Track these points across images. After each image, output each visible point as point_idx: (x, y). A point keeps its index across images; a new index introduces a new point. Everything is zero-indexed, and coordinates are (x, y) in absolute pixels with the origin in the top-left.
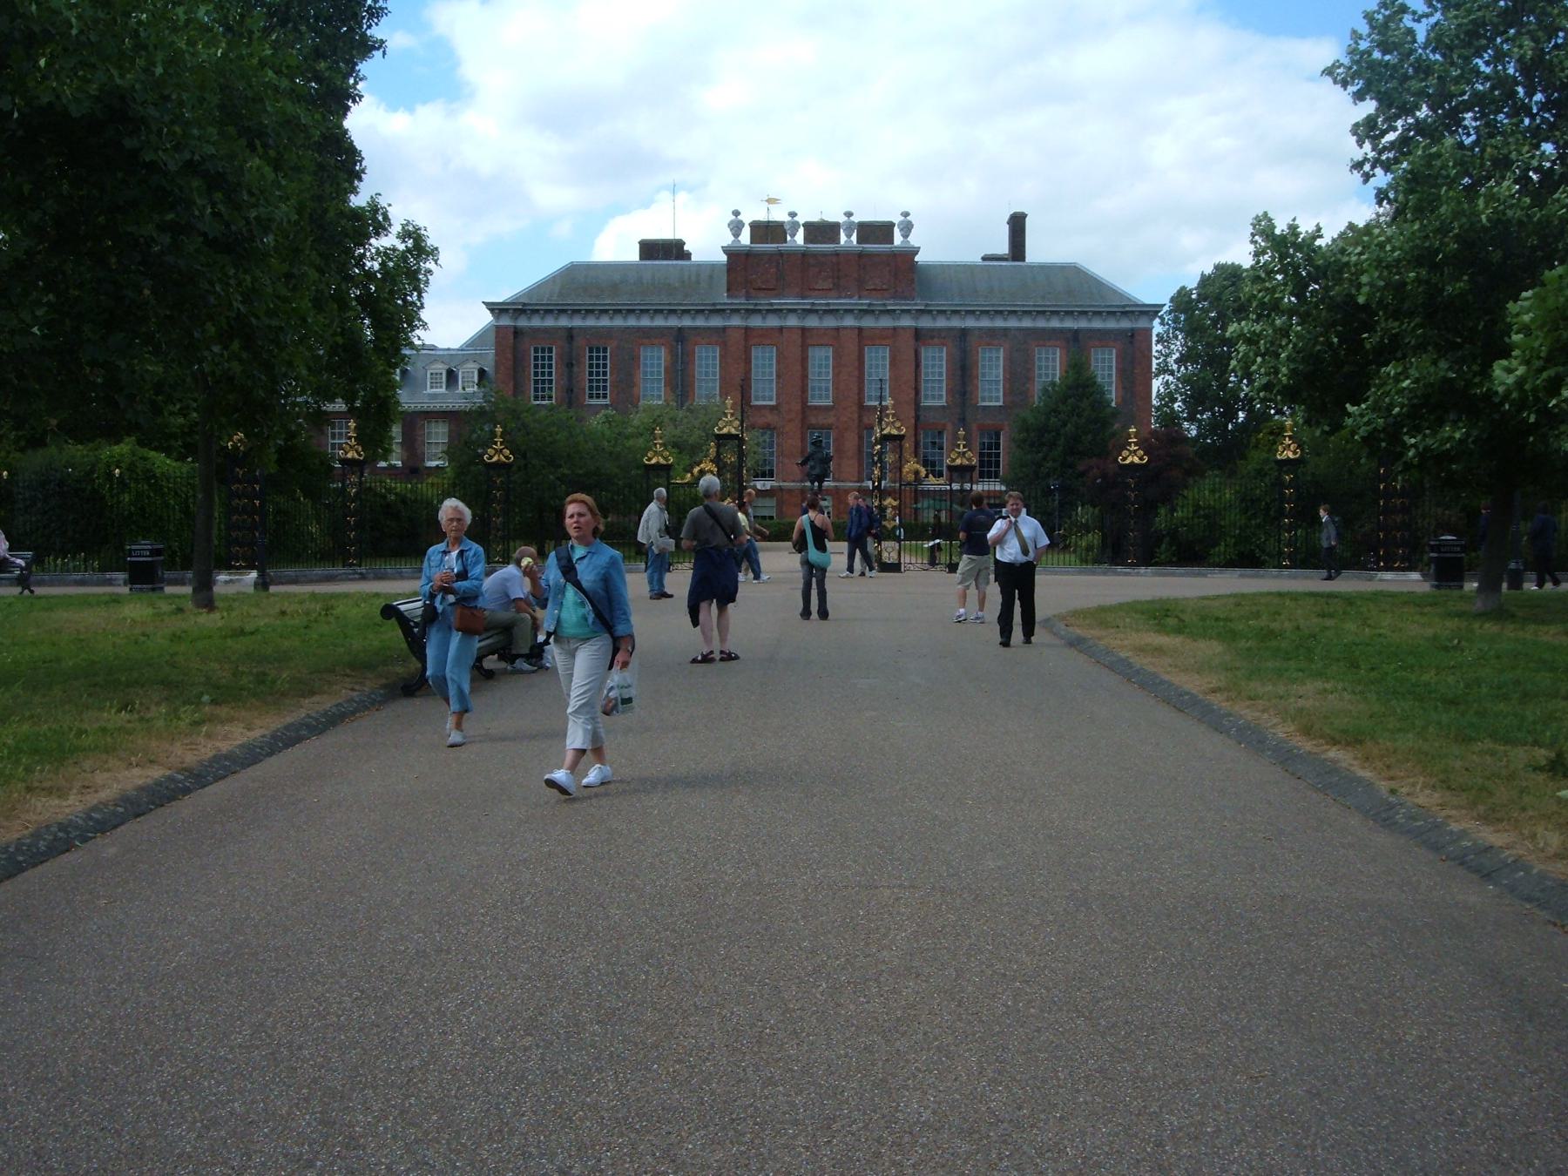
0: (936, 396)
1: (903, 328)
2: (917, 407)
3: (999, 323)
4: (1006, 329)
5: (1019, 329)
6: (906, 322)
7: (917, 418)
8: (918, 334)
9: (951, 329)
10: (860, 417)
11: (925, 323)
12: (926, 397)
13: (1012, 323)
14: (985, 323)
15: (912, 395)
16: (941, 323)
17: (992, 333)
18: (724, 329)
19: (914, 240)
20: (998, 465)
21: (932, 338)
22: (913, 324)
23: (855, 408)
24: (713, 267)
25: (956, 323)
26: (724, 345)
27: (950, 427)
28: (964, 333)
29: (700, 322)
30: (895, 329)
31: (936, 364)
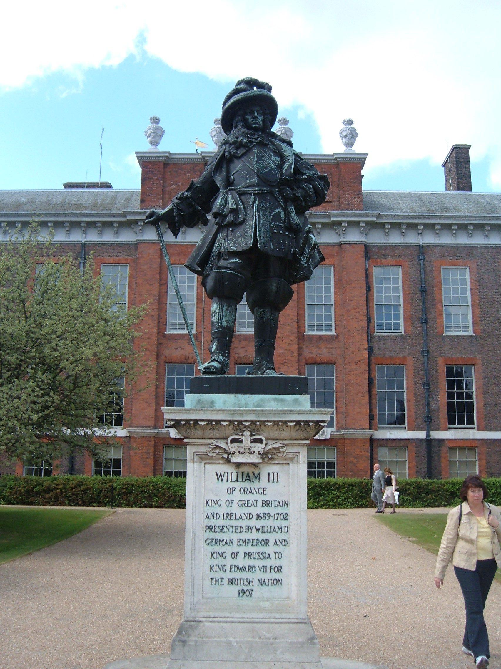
0: (394, 324)
1: (350, 244)
2: (370, 337)
3: (463, 240)
4: (471, 248)
5: (486, 247)
6: (354, 236)
7: (370, 351)
8: (368, 251)
9: (406, 246)
10: (299, 349)
11: (376, 238)
12: (380, 326)
13: (479, 240)
14: (446, 239)
15: (364, 323)
16: (395, 239)
17: (454, 250)
18: (136, 244)
19: (358, 148)
20: (470, 407)
21: (385, 256)
22: (363, 240)
23: (293, 338)
24: (133, 193)
25: (412, 239)
26: (135, 264)
27: (410, 361)
28: (422, 250)
29: (108, 237)
30: (340, 245)
31: (391, 285)
